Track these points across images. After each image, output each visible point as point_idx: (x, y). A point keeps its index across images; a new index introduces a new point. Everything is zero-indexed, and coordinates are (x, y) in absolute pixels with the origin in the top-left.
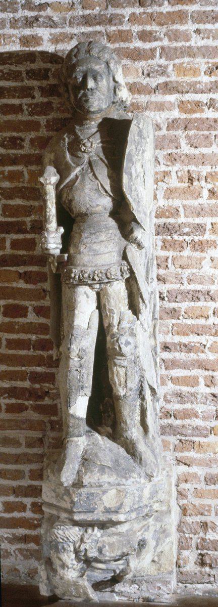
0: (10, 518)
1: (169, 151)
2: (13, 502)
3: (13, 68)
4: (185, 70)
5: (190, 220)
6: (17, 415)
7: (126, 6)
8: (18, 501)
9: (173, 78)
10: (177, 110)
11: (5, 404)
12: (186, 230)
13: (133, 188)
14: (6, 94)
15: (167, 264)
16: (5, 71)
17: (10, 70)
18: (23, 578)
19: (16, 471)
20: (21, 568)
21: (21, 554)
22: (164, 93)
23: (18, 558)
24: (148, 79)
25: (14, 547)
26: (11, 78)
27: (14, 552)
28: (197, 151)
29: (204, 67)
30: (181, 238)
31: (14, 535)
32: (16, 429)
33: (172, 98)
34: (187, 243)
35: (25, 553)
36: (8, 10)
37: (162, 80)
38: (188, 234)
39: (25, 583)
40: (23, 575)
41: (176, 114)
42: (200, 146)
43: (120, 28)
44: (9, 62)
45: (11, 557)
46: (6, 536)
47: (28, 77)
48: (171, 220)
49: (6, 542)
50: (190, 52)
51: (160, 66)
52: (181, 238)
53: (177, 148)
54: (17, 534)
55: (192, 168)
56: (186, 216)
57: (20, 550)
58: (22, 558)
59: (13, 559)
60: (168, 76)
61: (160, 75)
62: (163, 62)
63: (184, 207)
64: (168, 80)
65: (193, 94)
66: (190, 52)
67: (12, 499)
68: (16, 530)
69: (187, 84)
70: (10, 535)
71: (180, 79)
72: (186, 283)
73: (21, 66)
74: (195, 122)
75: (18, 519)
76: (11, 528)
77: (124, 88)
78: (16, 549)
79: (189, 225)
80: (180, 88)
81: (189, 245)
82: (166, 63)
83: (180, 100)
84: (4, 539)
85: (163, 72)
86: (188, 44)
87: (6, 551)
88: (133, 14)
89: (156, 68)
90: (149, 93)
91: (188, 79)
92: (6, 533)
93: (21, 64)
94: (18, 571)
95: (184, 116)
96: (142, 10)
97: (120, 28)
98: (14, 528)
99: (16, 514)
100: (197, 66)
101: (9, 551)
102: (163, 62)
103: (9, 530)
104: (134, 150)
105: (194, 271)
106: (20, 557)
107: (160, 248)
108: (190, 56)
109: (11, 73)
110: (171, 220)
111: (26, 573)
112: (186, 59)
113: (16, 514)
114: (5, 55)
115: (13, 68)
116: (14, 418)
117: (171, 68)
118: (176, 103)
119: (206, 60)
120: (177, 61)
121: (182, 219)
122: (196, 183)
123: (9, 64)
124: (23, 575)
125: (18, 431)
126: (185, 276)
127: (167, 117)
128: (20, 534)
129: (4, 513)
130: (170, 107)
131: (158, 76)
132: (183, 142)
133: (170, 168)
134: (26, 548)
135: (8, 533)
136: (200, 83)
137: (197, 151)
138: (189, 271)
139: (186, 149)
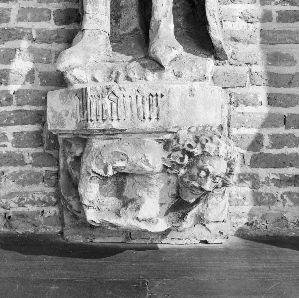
0: (278, 155)
2: (283, 135)
6: (291, 25)
8: (289, 134)
11: (277, 12)
18: (291, 228)
19: (289, 95)
20: (289, 216)
21: (291, 199)
23: (286, 204)
25: (282, 190)
27: (282, 197)
31: (281, 175)
32: (290, 43)
35: (295, 197)
39: (294, 234)
40: (292, 224)
45: (279, 203)
46: (271, 177)
49: (272, 184)
54: (285, 175)
57: (289, 194)
58: (292, 204)
59: (280, 205)
67: (282, 130)
68: (285, 169)
70: (277, 176)
75: (288, 156)
76: (280, 167)
78: (284, 194)
84: (270, 181)
87: (272, 195)
92: (272, 173)
94: (286, 220)
98: (283, 167)
99: (286, 150)
101: (275, 196)
103: (277, 171)
106: (289, 202)
111: (295, 222)
113: (286, 150)
116: (289, 29)
124: (292, 224)
125: (292, 45)
128: (289, 175)
129: (271, 148)
134: (297, 191)
135: (275, 174)
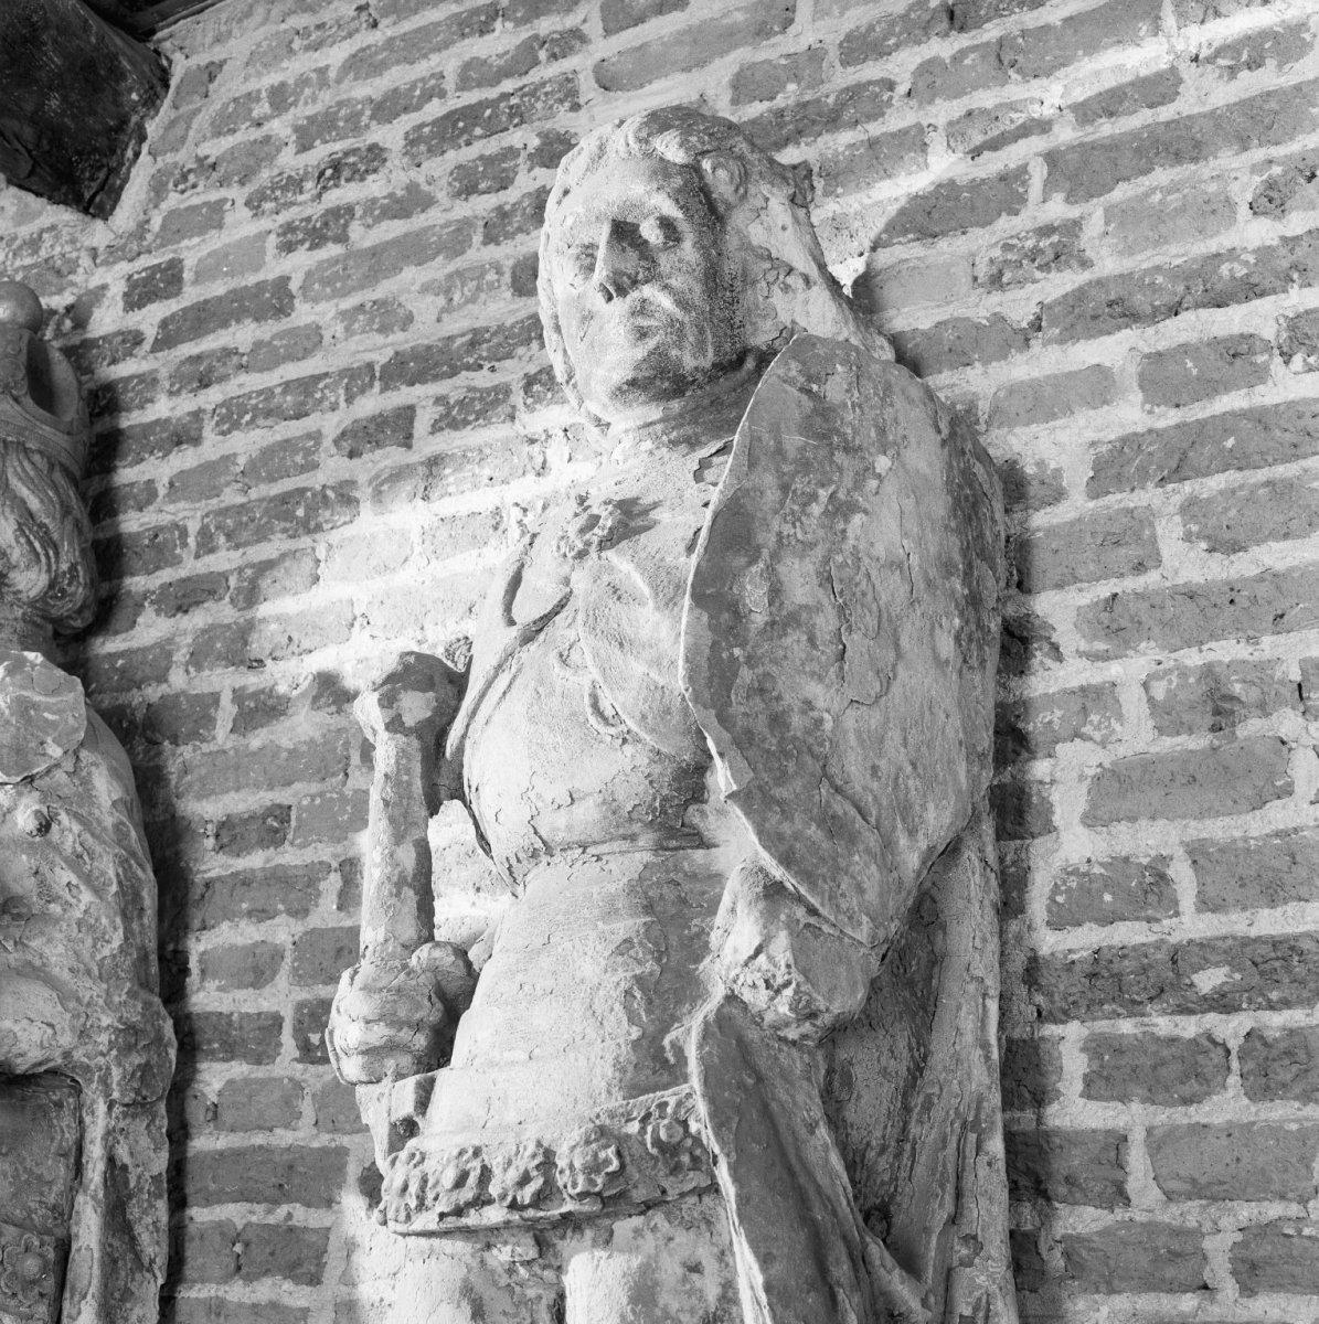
1: (1104, 590)
3: (483, 379)
4: (1159, 216)
5: (1236, 923)
7: (897, 46)
9: (1108, 264)
10: (1137, 396)
12: (1208, 980)
13: (746, 675)
14: (451, 479)
15: (1119, 1175)
16: (454, 397)
17: (471, 389)
22: (1070, 335)
24: (996, 297)
26: (471, 418)
28: (1243, 566)
29: (1245, 189)
30: (1189, 1027)
33: (1115, 349)
34: (1228, 1052)
36: (483, 186)
37: (1060, 284)
38: (1222, 1002)
41: (1130, 414)
42: (1259, 536)
43: (875, 129)
44: (471, 361)
47: (530, 401)
48: (1130, 933)
50: (1182, 144)
51: (1046, 230)
52: (1189, 1027)
53: (1140, 568)
55: (1226, 651)
56: (1206, 904)
60: (1085, 264)
61: (1045, 267)
62: (1057, 209)
63: (1198, 854)
64: (1083, 277)
65: (1205, 314)
66: (1182, 144)
69: (1175, 274)
71: (1143, 261)
72: (1229, 1289)
73: (508, 363)
74: (1227, 432)
77: (807, 280)
79: (1237, 951)
80: (1140, 301)
81: (1235, 1064)
82: (1074, 212)
83: (1147, 350)
85: (1060, 248)
86: (1166, 113)
88: (927, 68)
89: (1030, 244)
90: (1003, 354)
91: (1183, 251)
93: (509, 356)
95: (1169, 418)
96: (962, 41)
97: (875, 129)
100: (1212, 188)
102: (1057, 209)
104: (772, 496)
105: (1274, 1210)
107: (1079, 1086)
108: (1178, 158)
109: (473, 399)
110: (1130, 933)
112: (1162, 176)
114: (459, 341)
115: (483, 379)
117: (1095, 224)
118: (1133, 369)
119: (1258, 154)
120: (1121, 193)
121: (1191, 925)
122: (1251, 728)
123: (468, 368)
126: (1219, 1248)
127: (1091, 435)
130: (1099, 386)
131: (1038, 275)
132: (1169, 535)
133: (1114, 670)
136: (1232, 254)
137: (1243, 566)
138: (1246, 1212)
139: (1185, 562)
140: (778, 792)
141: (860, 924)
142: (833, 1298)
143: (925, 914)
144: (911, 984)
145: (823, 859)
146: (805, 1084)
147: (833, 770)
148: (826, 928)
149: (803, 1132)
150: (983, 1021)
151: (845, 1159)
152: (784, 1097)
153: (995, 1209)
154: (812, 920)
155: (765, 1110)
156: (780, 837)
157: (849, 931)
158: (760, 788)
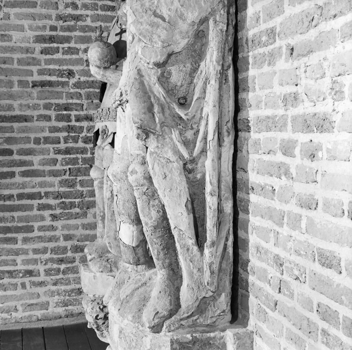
140: (141, 20)
141: (158, 44)
142: (154, 115)
143: (200, 35)
144: (195, 51)
145: (149, 32)
146: (154, 76)
147: (158, 11)
148: (149, 46)
149: (152, 85)
150: (212, 56)
151: (164, 89)
152: (147, 79)
153: (211, 95)
154: (146, 45)
155: (142, 83)
156: (140, 30)
157: (155, 45)
158: (137, 20)
